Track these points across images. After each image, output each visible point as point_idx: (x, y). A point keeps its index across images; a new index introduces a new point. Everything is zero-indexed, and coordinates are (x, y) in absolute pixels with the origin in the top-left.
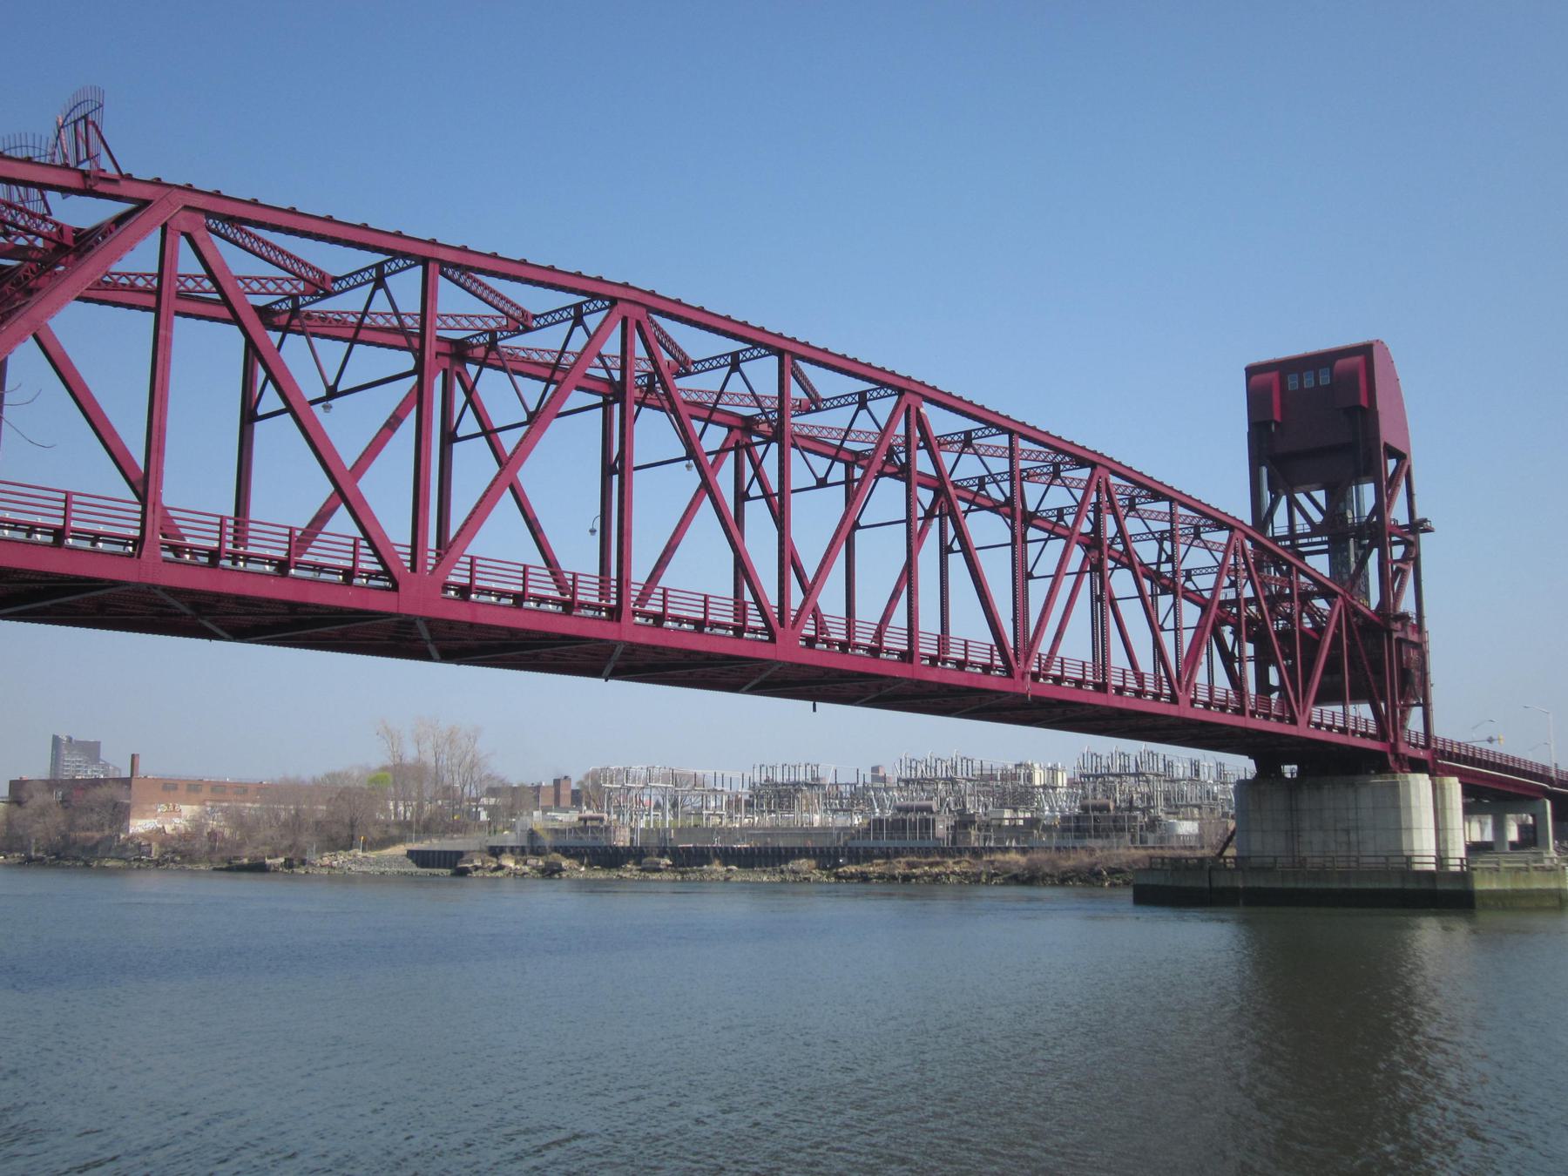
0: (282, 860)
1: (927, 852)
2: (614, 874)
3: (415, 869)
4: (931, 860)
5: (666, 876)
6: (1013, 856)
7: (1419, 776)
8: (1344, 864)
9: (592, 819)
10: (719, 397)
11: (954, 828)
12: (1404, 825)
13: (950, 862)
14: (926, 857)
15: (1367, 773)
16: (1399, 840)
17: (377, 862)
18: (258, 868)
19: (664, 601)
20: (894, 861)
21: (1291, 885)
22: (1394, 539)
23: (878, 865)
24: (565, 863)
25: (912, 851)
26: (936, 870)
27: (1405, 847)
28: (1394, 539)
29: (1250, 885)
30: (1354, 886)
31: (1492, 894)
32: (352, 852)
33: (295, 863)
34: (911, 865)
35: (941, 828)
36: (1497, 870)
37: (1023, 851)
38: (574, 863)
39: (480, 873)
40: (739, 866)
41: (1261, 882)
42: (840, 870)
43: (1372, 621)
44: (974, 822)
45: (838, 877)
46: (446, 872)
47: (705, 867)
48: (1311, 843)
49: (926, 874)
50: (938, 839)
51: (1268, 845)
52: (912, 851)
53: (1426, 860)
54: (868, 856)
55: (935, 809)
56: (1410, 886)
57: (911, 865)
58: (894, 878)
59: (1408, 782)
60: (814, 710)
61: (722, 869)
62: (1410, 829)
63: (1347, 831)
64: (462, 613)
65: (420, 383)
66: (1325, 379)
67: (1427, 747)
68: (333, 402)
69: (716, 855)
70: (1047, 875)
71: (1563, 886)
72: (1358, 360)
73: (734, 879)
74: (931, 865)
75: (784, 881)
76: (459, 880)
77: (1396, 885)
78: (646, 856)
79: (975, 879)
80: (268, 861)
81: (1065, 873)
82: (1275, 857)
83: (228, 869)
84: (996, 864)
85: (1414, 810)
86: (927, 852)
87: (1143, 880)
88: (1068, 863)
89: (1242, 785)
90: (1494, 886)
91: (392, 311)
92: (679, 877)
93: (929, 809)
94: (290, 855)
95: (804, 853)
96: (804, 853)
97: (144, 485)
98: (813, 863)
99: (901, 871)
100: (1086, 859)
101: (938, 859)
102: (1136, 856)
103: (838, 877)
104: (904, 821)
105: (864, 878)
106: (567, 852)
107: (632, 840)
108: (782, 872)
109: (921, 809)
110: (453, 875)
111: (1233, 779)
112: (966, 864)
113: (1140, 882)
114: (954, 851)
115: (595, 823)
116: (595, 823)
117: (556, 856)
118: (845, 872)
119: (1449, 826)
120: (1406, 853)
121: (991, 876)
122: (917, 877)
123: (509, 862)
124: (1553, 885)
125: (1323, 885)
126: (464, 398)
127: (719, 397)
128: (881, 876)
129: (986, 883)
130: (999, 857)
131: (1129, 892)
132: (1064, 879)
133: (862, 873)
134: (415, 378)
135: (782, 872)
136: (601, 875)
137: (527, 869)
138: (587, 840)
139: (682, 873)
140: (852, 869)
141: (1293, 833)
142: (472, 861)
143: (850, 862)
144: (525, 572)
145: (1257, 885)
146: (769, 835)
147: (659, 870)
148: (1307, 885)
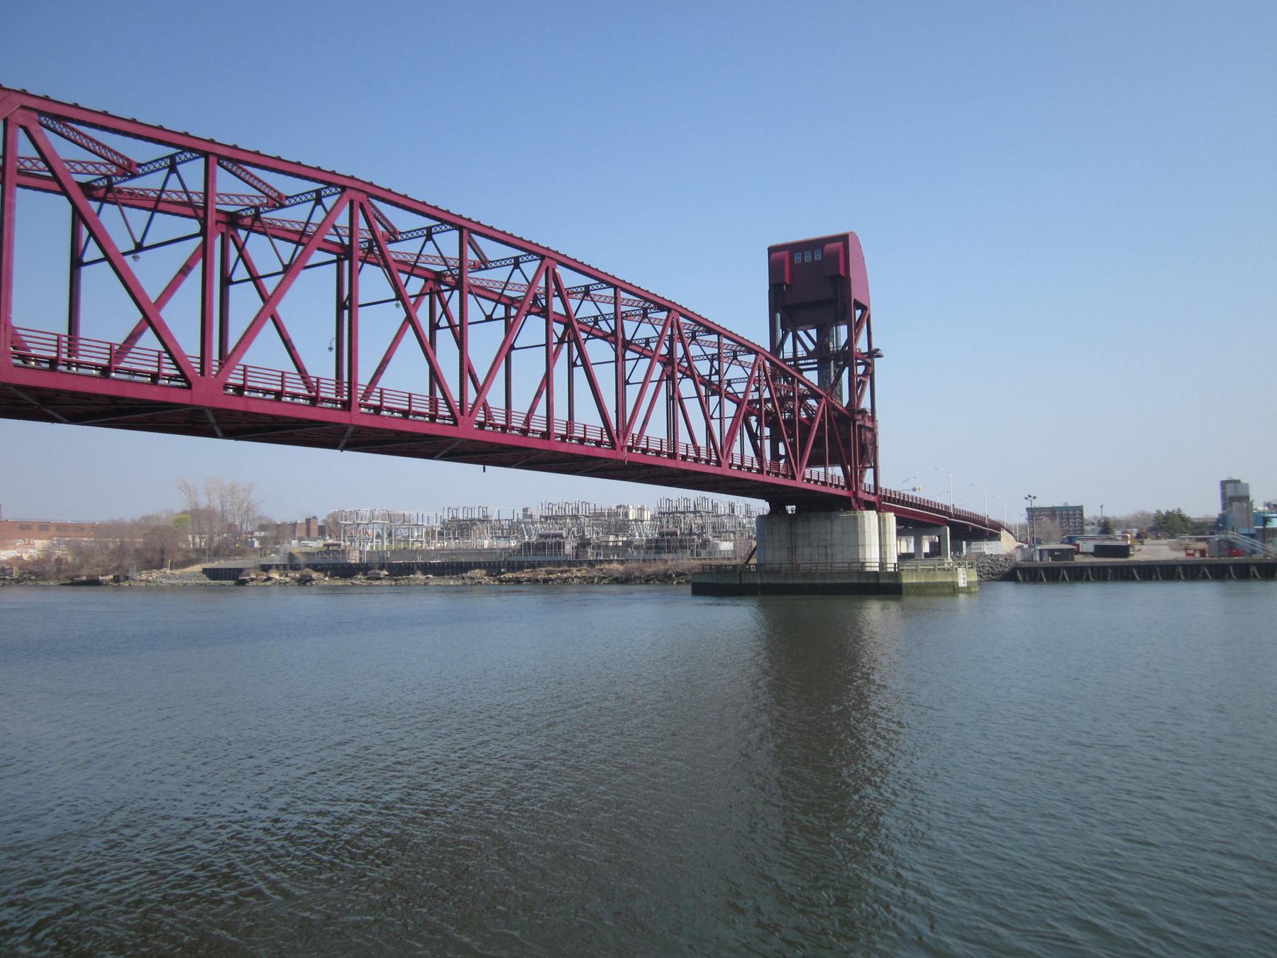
0: (111, 577)
1: (559, 564)
2: (349, 582)
3: (208, 581)
4: (561, 569)
5: (384, 582)
6: (615, 566)
7: (870, 512)
8: (824, 568)
9: (333, 545)
10: (418, 257)
11: (577, 548)
13: (574, 570)
14: (559, 567)
15: (839, 510)
17: (181, 577)
18: (93, 583)
19: (381, 397)
20: (538, 570)
21: (790, 581)
23: (527, 573)
24: (315, 575)
25: (549, 563)
26: (565, 575)
28: (859, 361)
29: (765, 581)
30: (829, 581)
31: (912, 585)
32: (162, 570)
33: (121, 578)
34: (550, 573)
35: (568, 548)
36: (916, 570)
37: (622, 562)
38: (321, 575)
39: (254, 583)
40: (434, 575)
41: (772, 581)
43: (844, 413)
44: (590, 544)
45: (501, 581)
46: (231, 582)
47: (411, 576)
48: (803, 555)
49: (558, 578)
50: (567, 555)
51: (776, 556)
52: (549, 563)
53: (873, 565)
54: (520, 567)
55: (564, 535)
56: (863, 581)
57: (550, 573)
58: (537, 581)
59: (863, 516)
60: (484, 471)
61: (423, 577)
62: (864, 545)
63: (826, 547)
64: (238, 405)
65: (204, 244)
66: (818, 257)
67: (875, 493)
68: (140, 254)
69: (419, 568)
70: (637, 577)
71: (955, 580)
72: (839, 244)
73: (431, 583)
74: (562, 572)
75: (464, 584)
76: (241, 588)
77: (855, 581)
78: (371, 569)
79: (590, 581)
80: (101, 578)
81: (648, 576)
82: (781, 564)
83: (71, 584)
84: (604, 571)
85: (866, 534)
86: (559, 564)
87: (698, 580)
88: (650, 569)
89: (760, 518)
90: (915, 581)
92: (393, 583)
93: (561, 536)
94: (117, 574)
95: (478, 565)
96: (478, 565)
98: (484, 572)
100: (660, 567)
101: (567, 568)
102: (694, 565)
103: (501, 581)
104: (544, 544)
105: (518, 581)
106: (316, 568)
107: (361, 559)
108: (463, 578)
109: (555, 536)
110: (235, 584)
111: (755, 515)
112: (584, 571)
113: (697, 581)
114: (577, 562)
115: (335, 548)
116: (335, 548)
117: (308, 571)
119: (888, 543)
120: (861, 561)
121: (601, 579)
122: (552, 580)
123: (275, 575)
124: (950, 580)
125: (809, 581)
127: (418, 257)
128: (529, 580)
129: (598, 583)
130: (606, 566)
131: (689, 588)
132: (648, 580)
133: (517, 578)
134: (200, 239)
135: (463, 578)
136: (340, 583)
137: (288, 579)
138: (330, 559)
139: (396, 580)
140: (510, 575)
141: (792, 549)
142: (249, 575)
143: (508, 571)
144: (283, 376)
145: (769, 582)
146: (455, 554)
147: (379, 579)
148: (800, 581)
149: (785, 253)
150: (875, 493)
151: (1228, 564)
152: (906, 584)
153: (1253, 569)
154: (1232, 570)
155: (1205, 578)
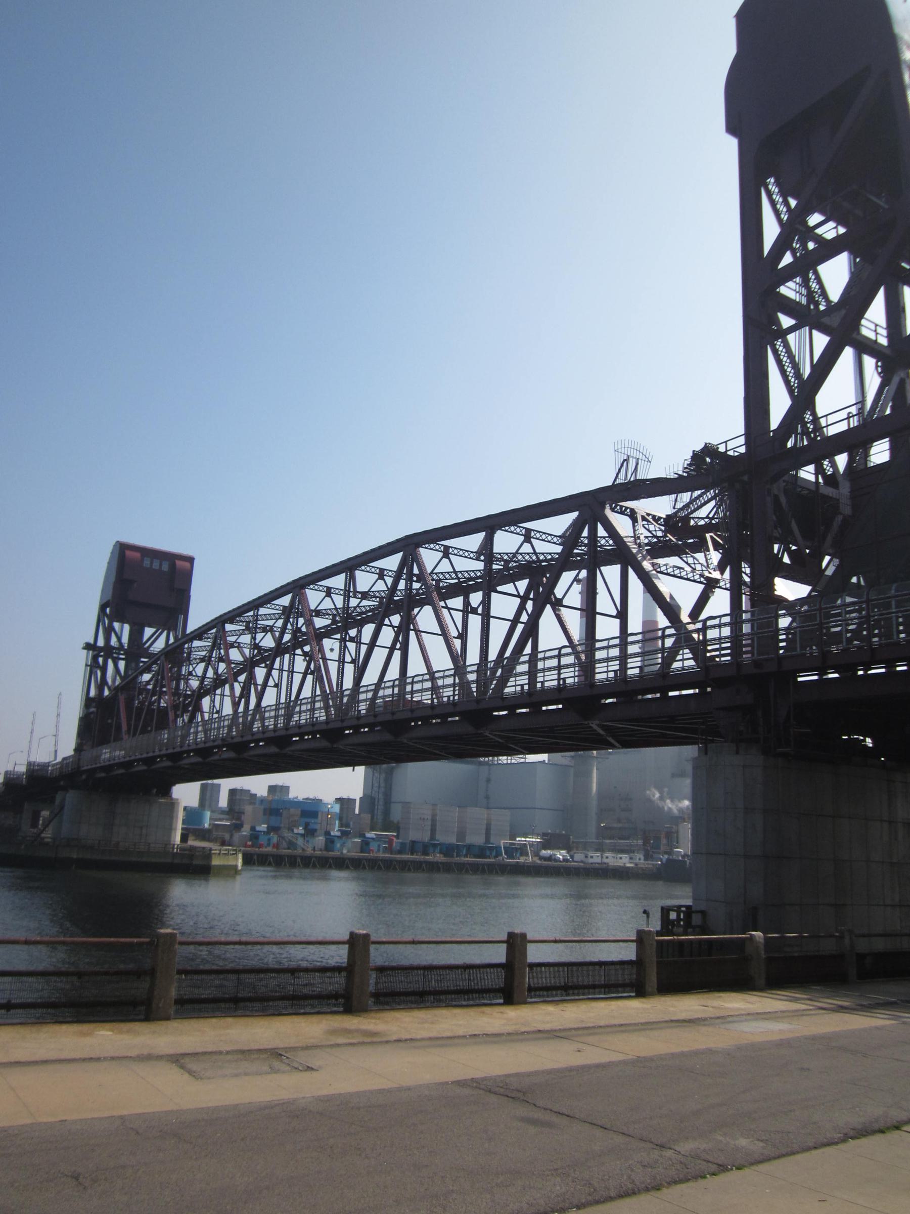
12: (174, 827)
16: (169, 836)
22: (122, 652)
27: (172, 839)
28: (122, 652)
30: (144, 859)
63: (141, 828)
72: (187, 565)
77: (169, 860)
91: (533, 552)
149: (137, 555)
151: (284, 855)
152: (214, 865)
153: (299, 860)
154: (286, 860)
155: (270, 864)
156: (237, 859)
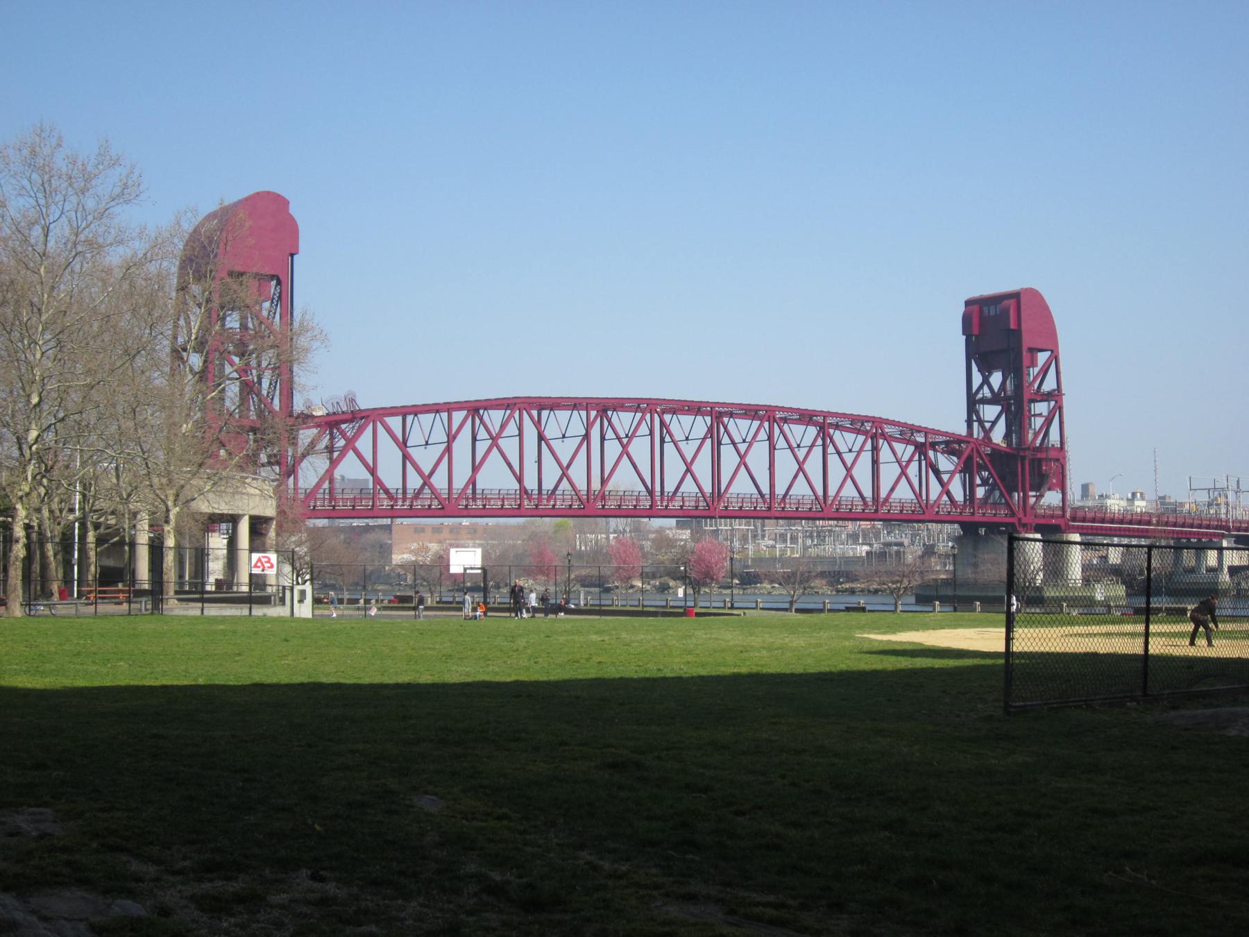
7: (1075, 535)
33: (501, 585)
42: (839, 586)
45: (838, 591)
47: (759, 585)
55: (906, 544)
58: (869, 591)
61: (769, 586)
68: (427, 446)
72: (1012, 302)
87: (919, 592)
92: (741, 593)
93: (901, 544)
97: (373, 471)
98: (824, 582)
99: (874, 587)
103: (838, 591)
109: (896, 544)
117: (666, 579)
118: (842, 588)
122: (882, 591)
126: (479, 422)
128: (862, 591)
133: (852, 588)
134: (446, 444)
137: (648, 587)
139: (744, 589)
150: (1063, 516)
156: (1094, 589)
